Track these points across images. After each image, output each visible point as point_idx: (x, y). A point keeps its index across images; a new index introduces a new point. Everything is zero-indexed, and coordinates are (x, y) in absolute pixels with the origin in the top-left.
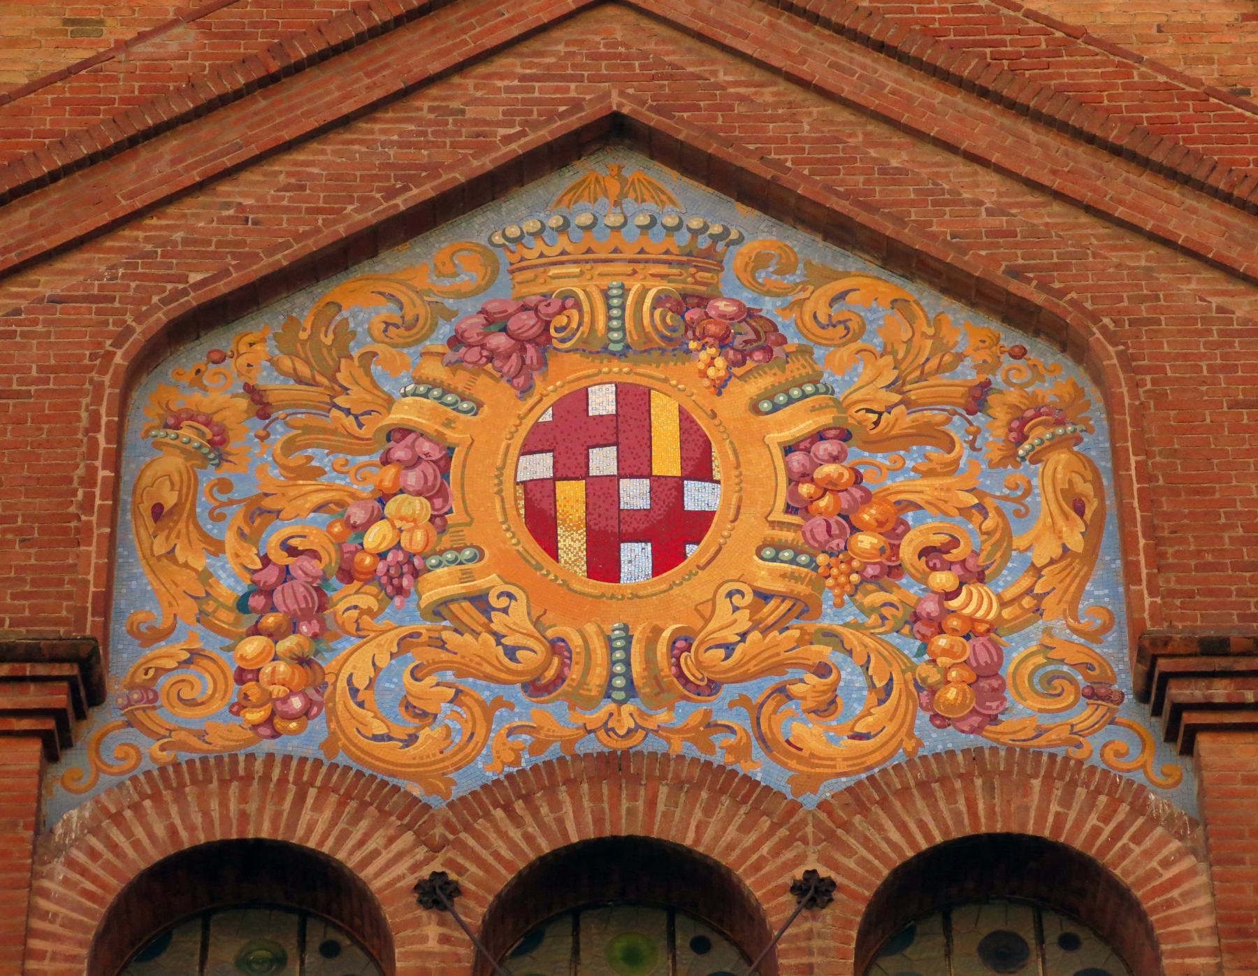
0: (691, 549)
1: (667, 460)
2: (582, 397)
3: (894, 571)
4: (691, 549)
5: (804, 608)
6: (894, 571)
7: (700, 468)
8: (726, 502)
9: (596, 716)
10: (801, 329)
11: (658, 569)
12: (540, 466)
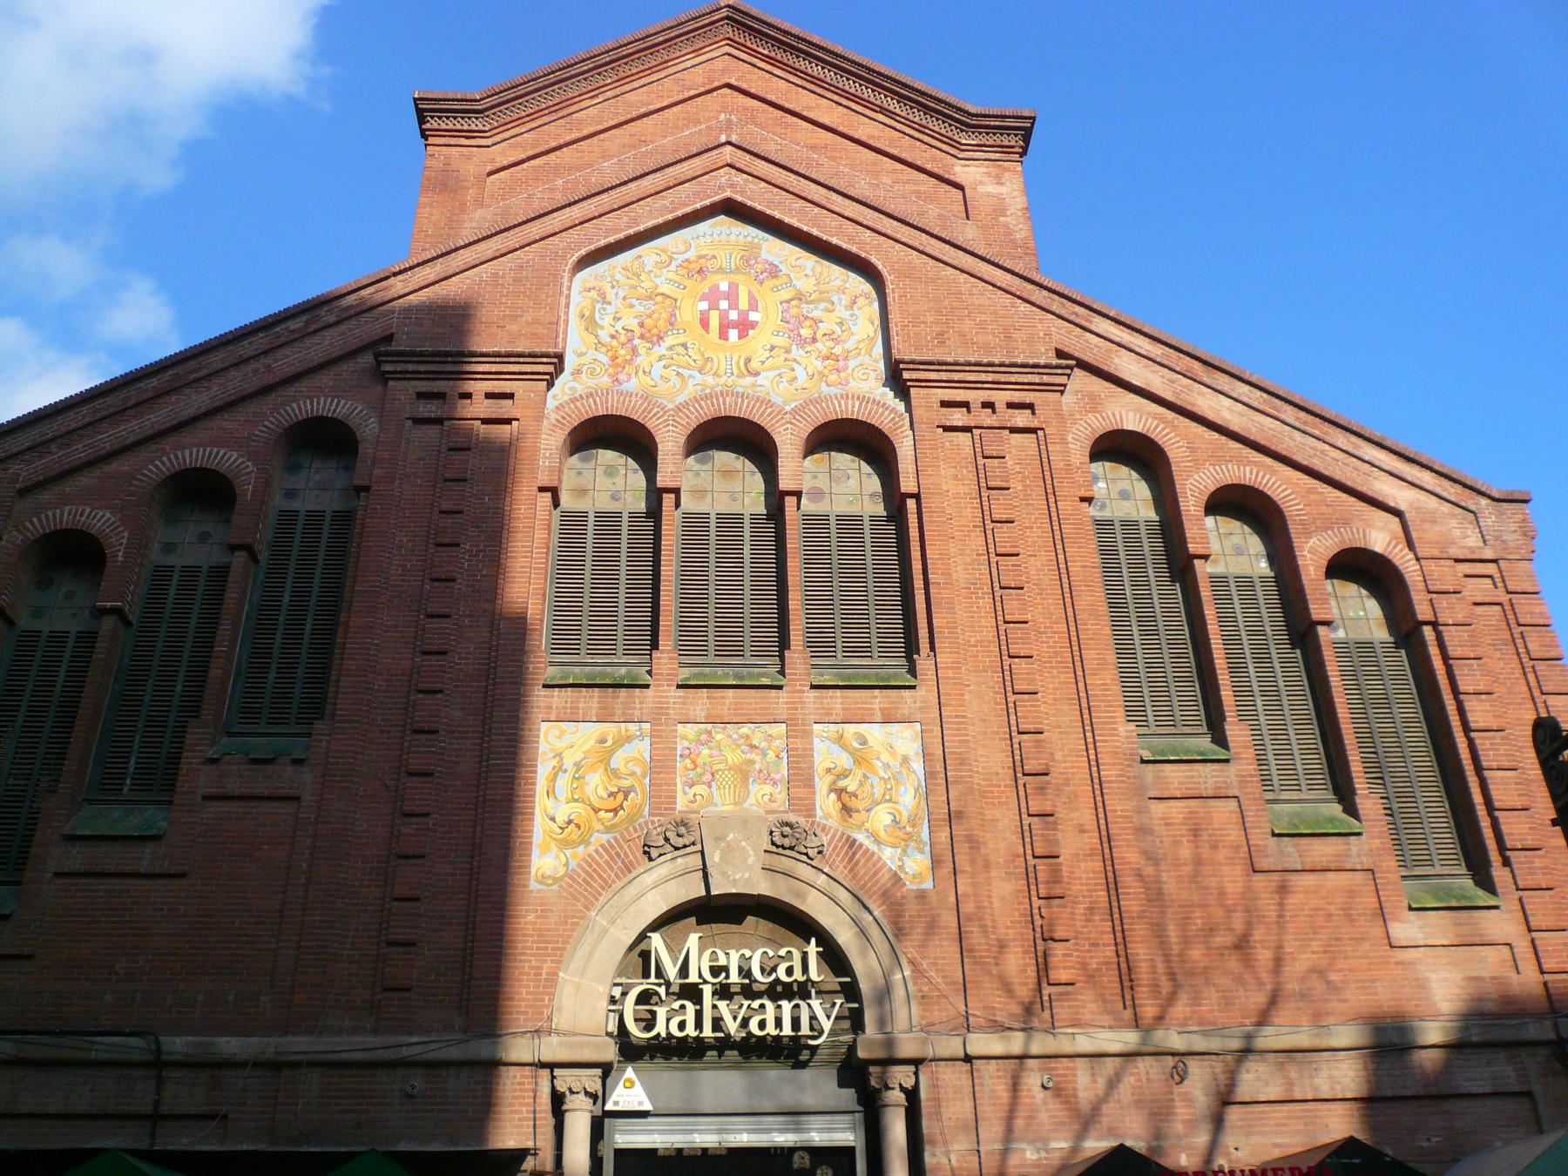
0: (751, 332)
1: (743, 303)
2: (717, 287)
3: (814, 340)
4: (751, 332)
5: (788, 351)
6: (814, 340)
7: (753, 306)
8: (762, 319)
9: (722, 380)
10: (787, 267)
11: (740, 337)
12: (704, 305)
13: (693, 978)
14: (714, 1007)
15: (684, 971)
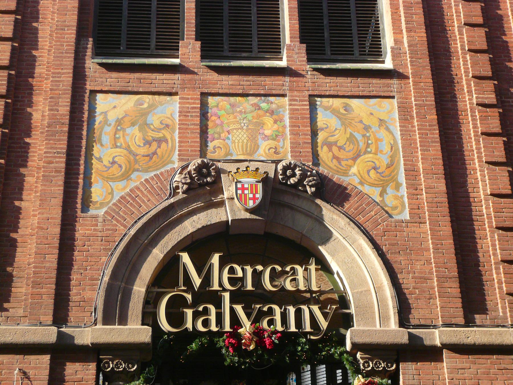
13: (216, 287)
14: (232, 310)
15: (207, 280)
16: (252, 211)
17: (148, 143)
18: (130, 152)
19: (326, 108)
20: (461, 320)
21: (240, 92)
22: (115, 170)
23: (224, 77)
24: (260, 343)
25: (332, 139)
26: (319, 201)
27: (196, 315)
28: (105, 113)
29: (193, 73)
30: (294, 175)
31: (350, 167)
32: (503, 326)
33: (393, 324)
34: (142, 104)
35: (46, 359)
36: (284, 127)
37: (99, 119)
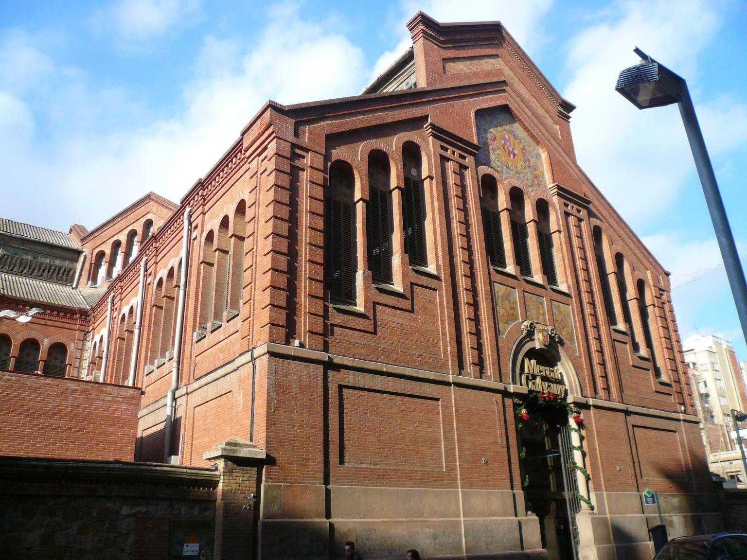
16: (545, 345)
17: (511, 309)
18: (507, 312)
19: (555, 305)
20: (594, 396)
21: (532, 292)
22: (504, 319)
23: (528, 285)
24: (549, 398)
25: (558, 319)
26: (558, 344)
27: (534, 383)
28: (497, 292)
29: (519, 280)
30: (553, 333)
31: (563, 331)
32: (601, 399)
33: (580, 396)
34: (507, 291)
35: (500, 395)
36: (545, 311)
37: (496, 294)
